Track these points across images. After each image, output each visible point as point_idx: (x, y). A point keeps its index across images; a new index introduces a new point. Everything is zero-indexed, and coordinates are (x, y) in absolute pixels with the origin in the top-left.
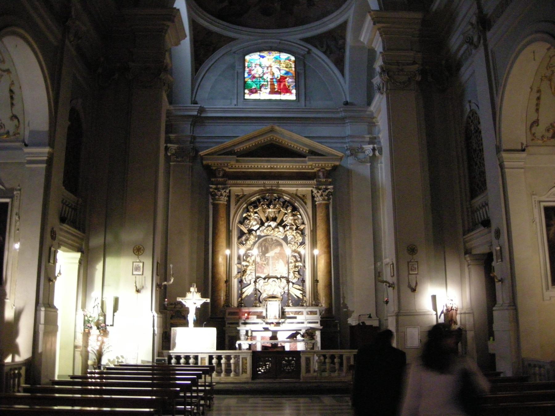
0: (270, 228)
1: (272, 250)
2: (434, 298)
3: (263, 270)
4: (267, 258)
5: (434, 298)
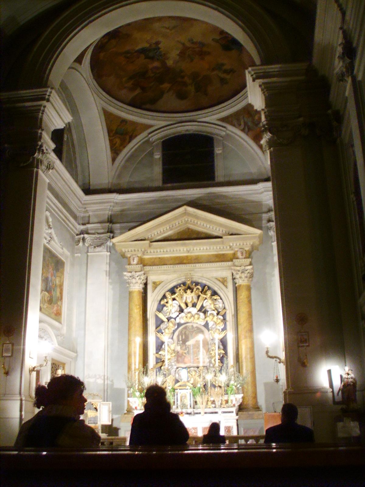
0: (189, 315)
1: (193, 338)
2: (329, 372)
3: (184, 359)
4: (188, 347)
5: (329, 372)
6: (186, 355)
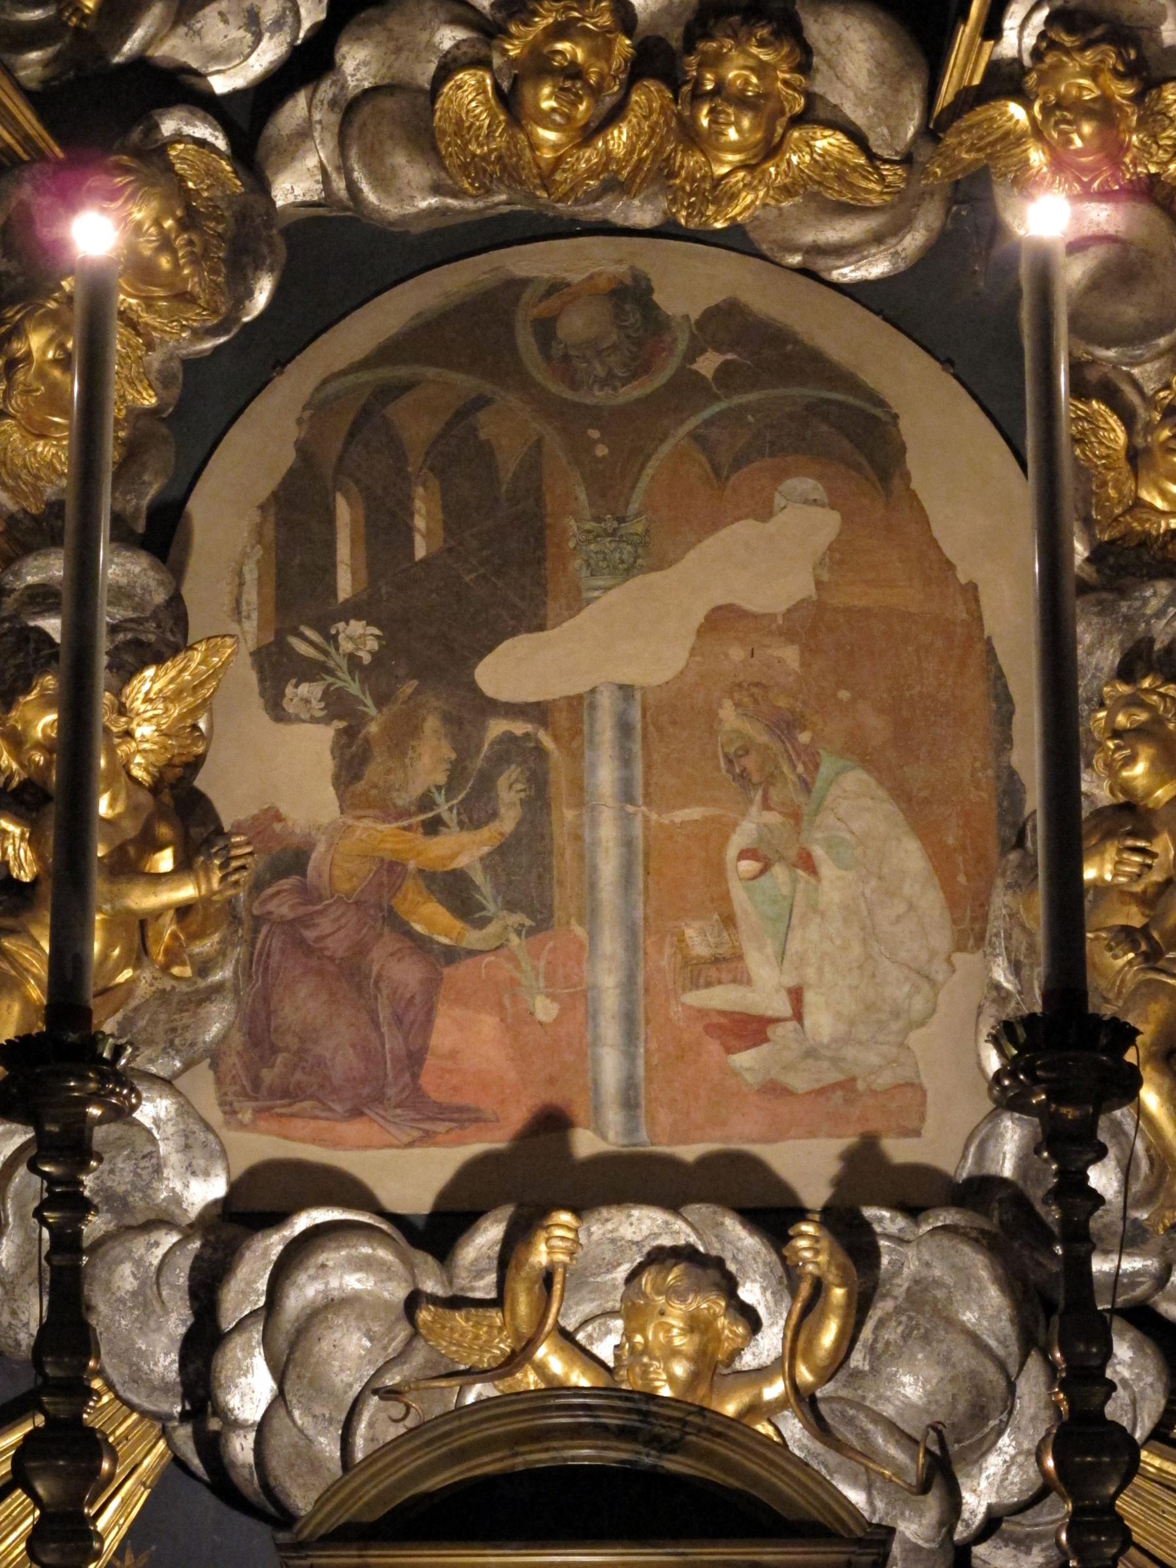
6: (473, 938)
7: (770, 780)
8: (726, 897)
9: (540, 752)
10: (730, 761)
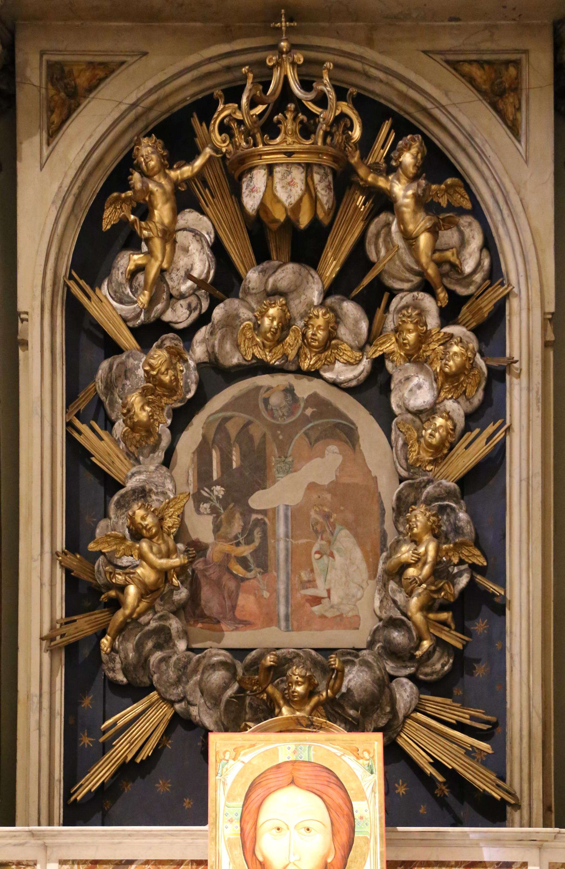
1: (290, 469)
4: (257, 522)
7: (323, 531)
8: (311, 564)
9: (265, 523)
10: (313, 526)
